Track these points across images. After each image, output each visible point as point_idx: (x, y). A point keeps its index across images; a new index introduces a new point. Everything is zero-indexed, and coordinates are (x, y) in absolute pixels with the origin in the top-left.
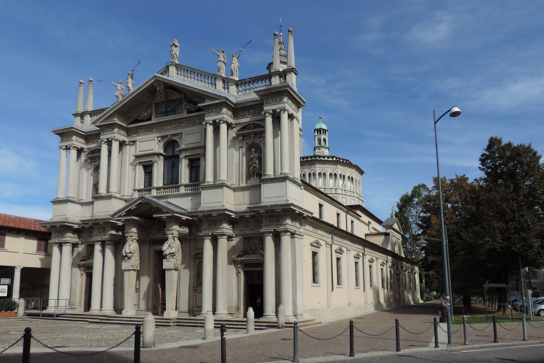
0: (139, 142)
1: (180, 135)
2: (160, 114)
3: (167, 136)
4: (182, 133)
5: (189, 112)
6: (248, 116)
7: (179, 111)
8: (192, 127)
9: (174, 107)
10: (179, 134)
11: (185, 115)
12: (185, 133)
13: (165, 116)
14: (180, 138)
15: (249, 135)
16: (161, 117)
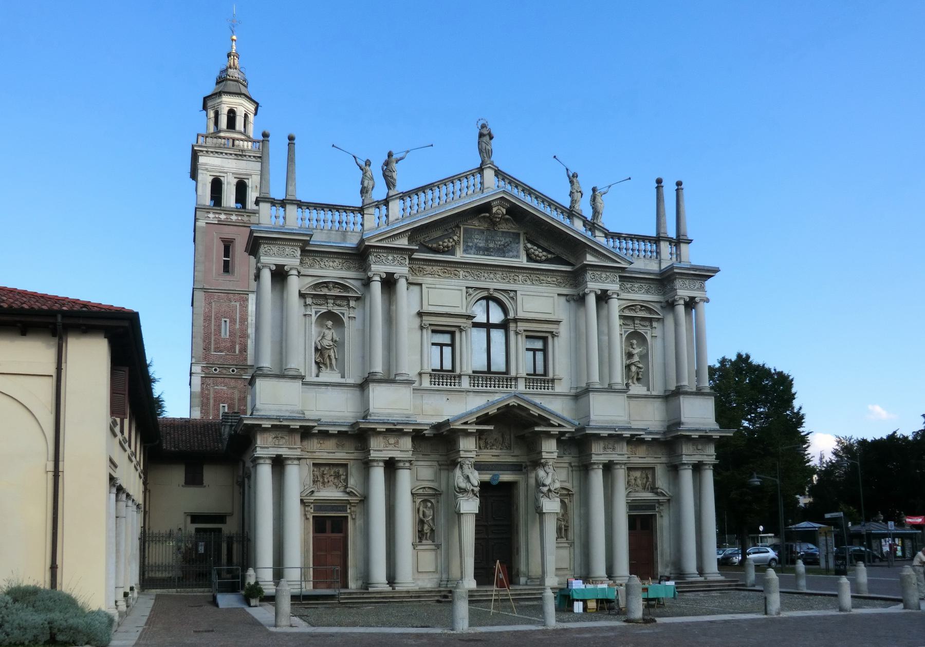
0: (427, 287)
1: (512, 294)
2: (473, 249)
3: (488, 289)
4: (516, 291)
5: (530, 258)
6: (630, 290)
7: (511, 254)
8: (537, 285)
9: (504, 245)
10: (511, 291)
11: (523, 261)
12: (523, 293)
13: (484, 255)
14: (512, 298)
15: (632, 319)
16: (474, 254)
